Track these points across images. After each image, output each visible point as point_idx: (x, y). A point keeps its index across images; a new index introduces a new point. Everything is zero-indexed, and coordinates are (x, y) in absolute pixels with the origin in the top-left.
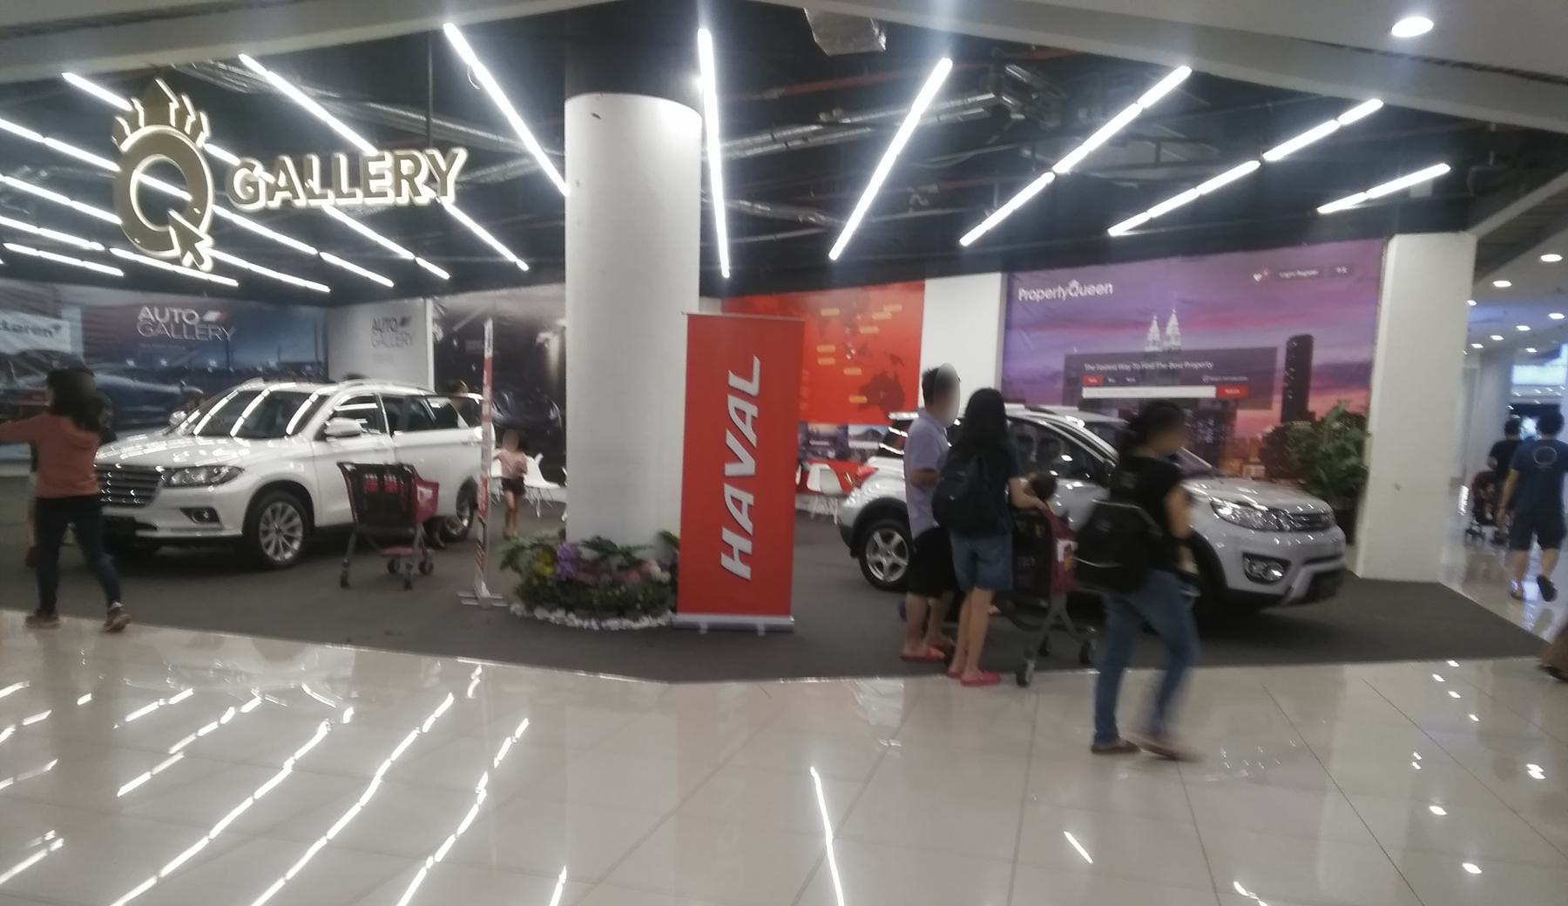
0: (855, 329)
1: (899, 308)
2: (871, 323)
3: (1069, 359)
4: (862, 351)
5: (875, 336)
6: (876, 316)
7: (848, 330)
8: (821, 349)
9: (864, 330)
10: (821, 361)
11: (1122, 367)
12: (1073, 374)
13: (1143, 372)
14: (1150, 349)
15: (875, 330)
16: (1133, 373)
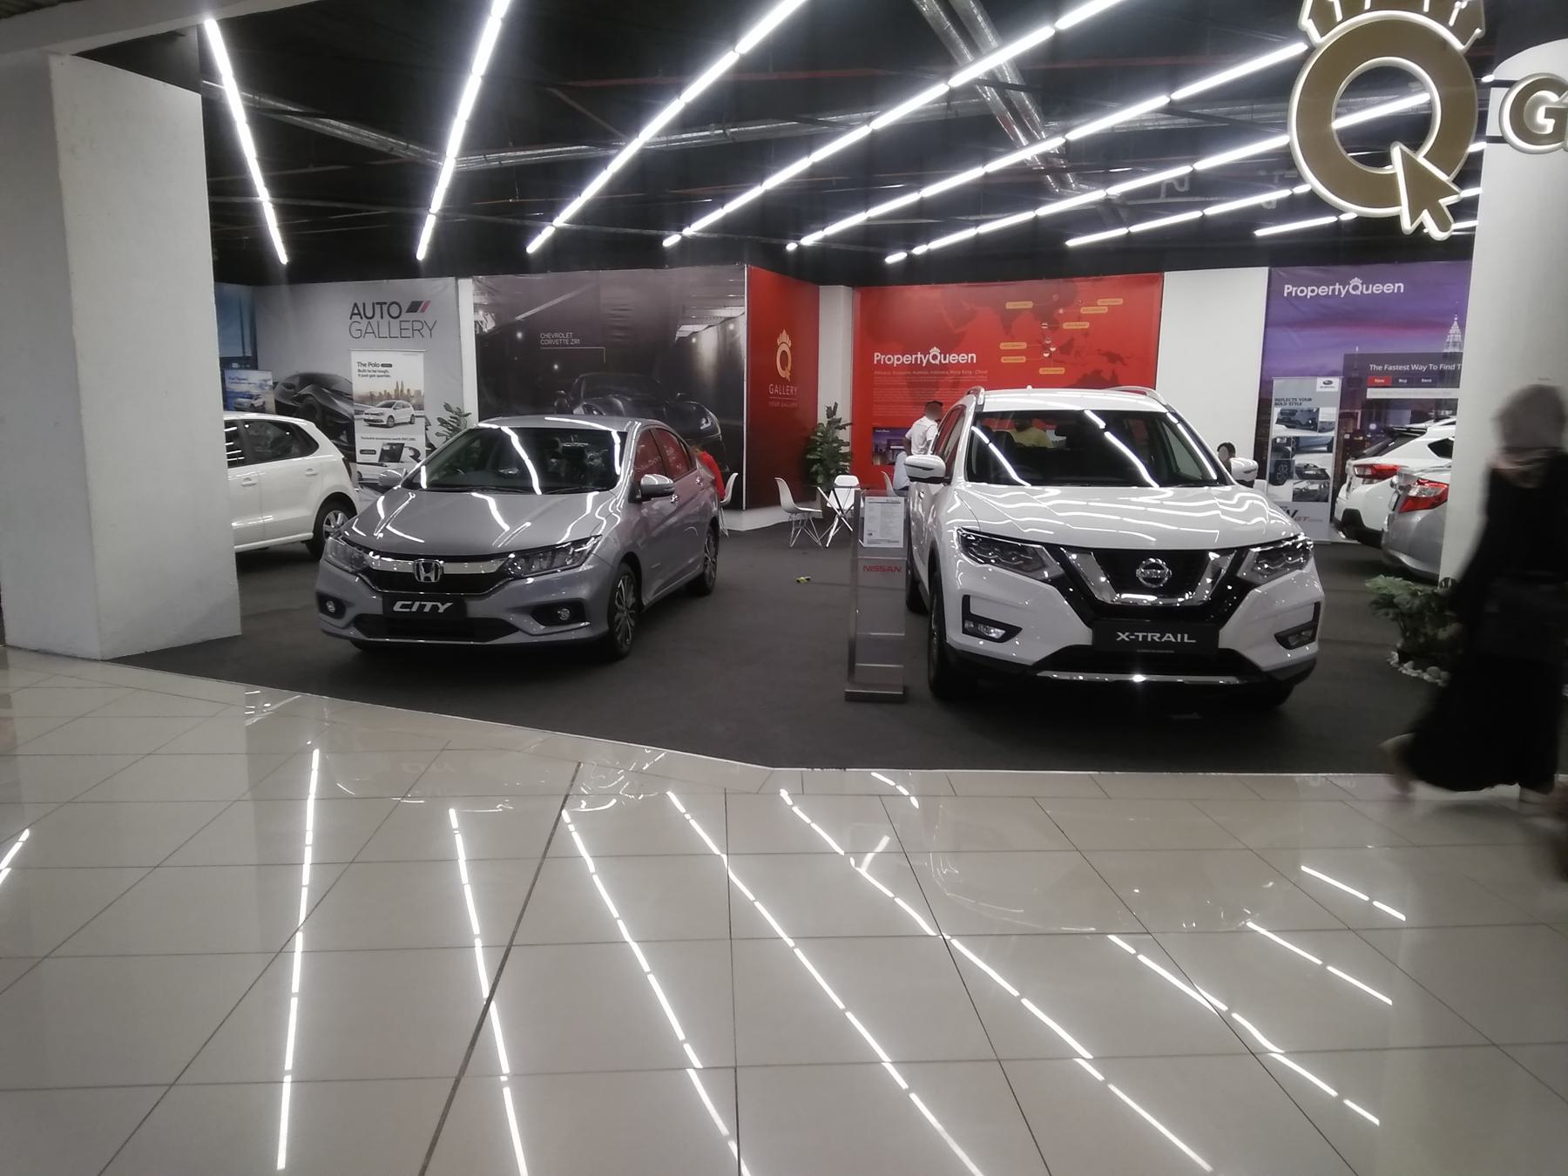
0: (1055, 326)
1: (1120, 301)
2: (1080, 318)
3: (1348, 358)
4: (1065, 348)
5: (1085, 333)
6: (1084, 310)
7: (1045, 326)
8: (1004, 346)
9: (1066, 326)
10: (1004, 360)
11: (1415, 367)
12: (1355, 375)
13: (1442, 373)
14: (1450, 350)
15: (1086, 325)
16: (1428, 374)
